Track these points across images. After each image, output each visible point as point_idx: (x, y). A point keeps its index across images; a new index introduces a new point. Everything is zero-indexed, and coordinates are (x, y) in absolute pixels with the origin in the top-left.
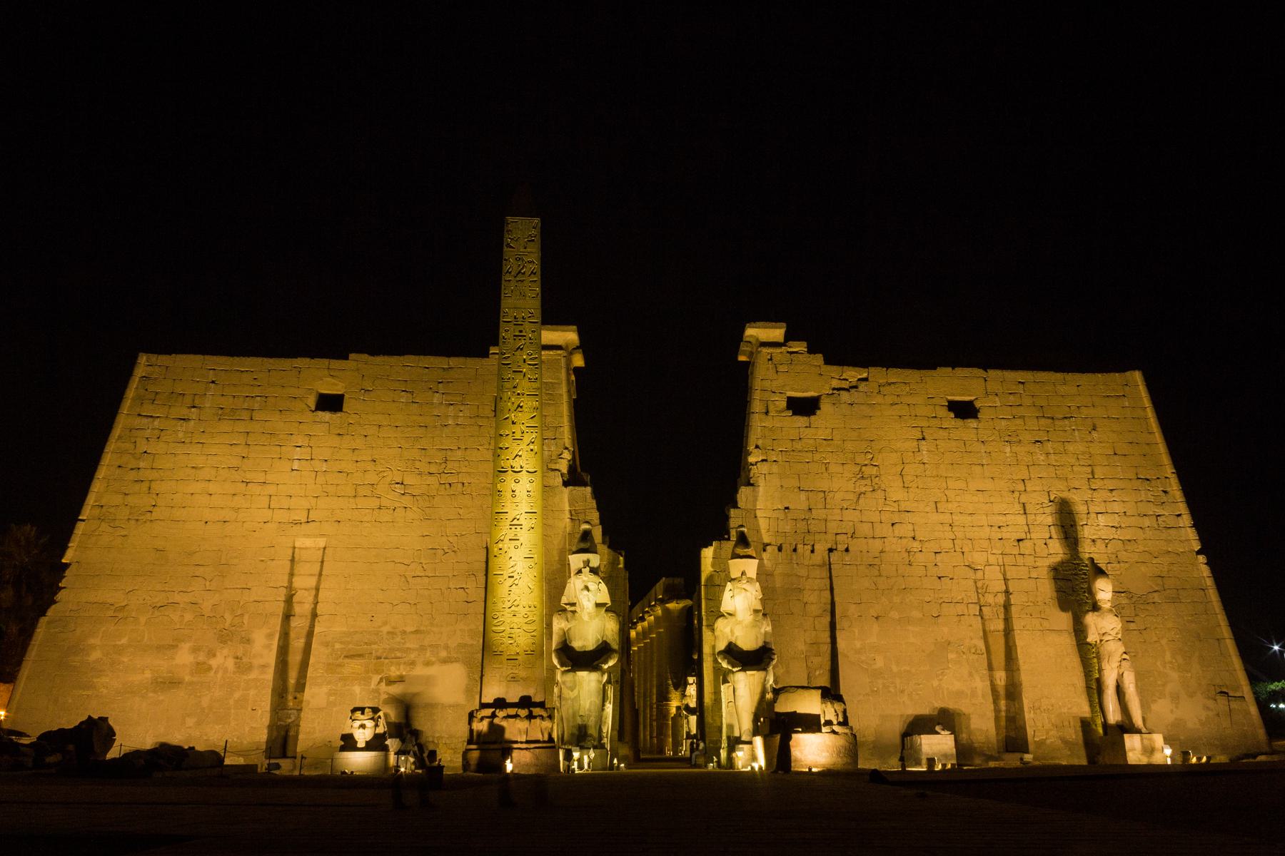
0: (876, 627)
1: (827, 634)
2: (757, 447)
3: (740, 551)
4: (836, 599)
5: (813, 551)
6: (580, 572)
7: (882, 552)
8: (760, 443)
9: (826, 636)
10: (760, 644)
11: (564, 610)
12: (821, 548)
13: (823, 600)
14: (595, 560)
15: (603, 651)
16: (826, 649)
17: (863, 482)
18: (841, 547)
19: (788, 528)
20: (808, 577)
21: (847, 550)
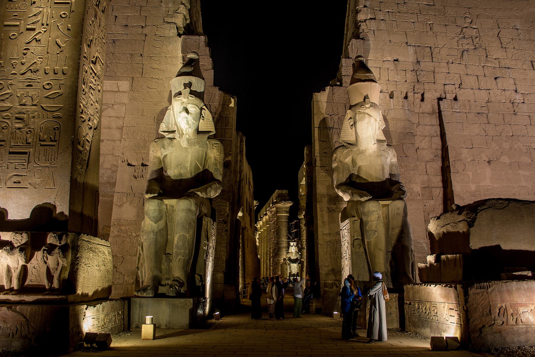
0: (488, 171)
1: (439, 178)
2: (365, 6)
3: (359, 75)
4: (449, 143)
5: (422, 100)
6: (180, 94)
7: (488, 102)
8: (368, 3)
9: (437, 181)
10: (387, 176)
11: (163, 137)
12: (431, 96)
13: (434, 146)
14: (198, 85)
15: (203, 178)
16: (438, 193)
17: (465, 41)
18: (450, 96)
19: (398, 78)
20: (419, 124)
21: (455, 99)
